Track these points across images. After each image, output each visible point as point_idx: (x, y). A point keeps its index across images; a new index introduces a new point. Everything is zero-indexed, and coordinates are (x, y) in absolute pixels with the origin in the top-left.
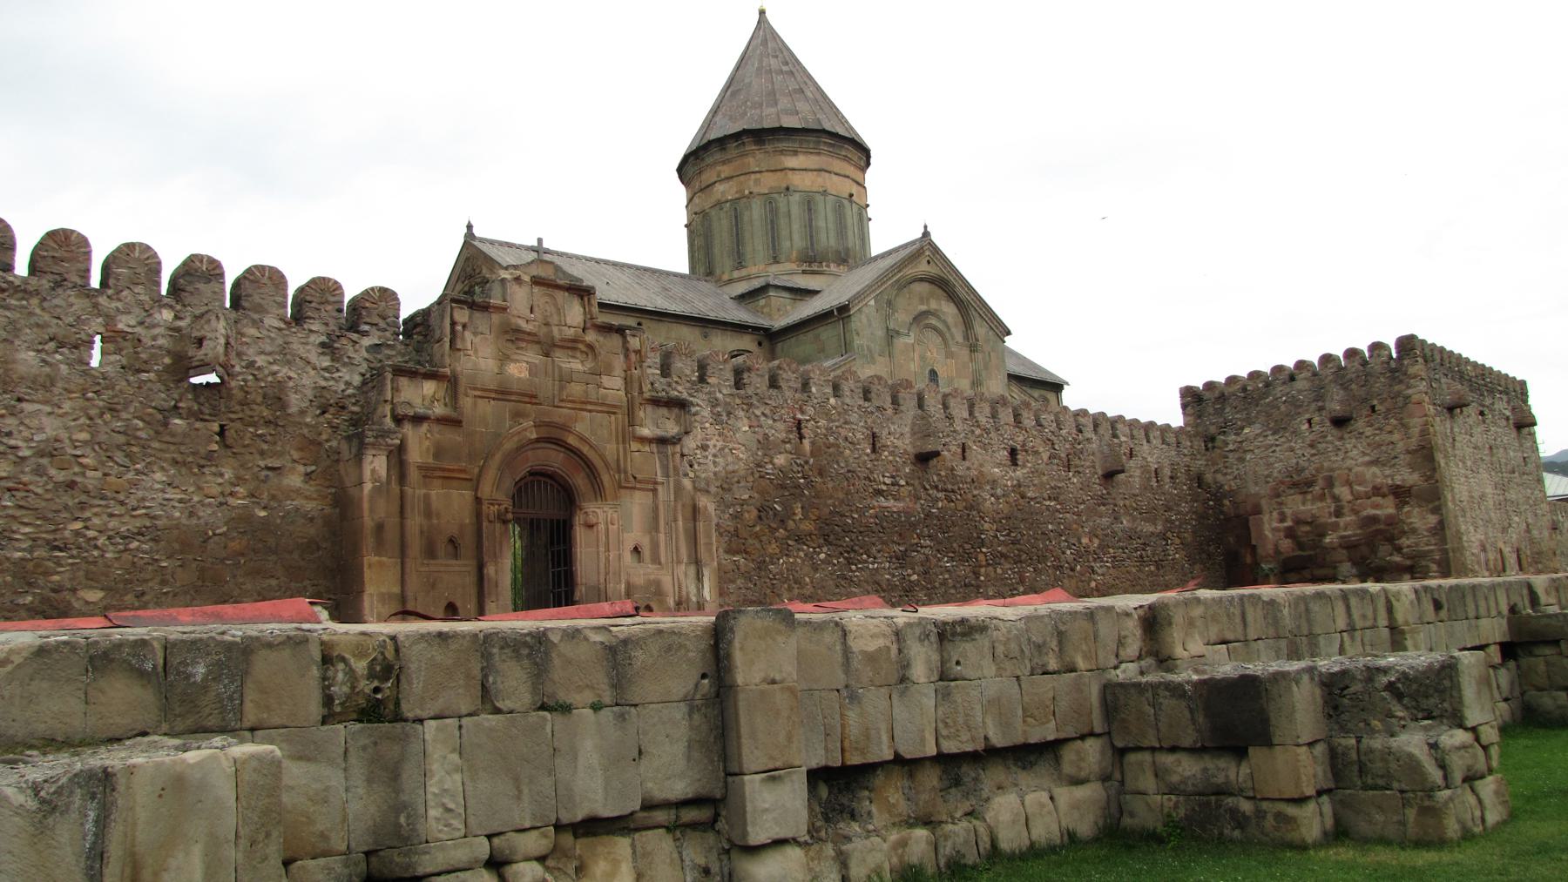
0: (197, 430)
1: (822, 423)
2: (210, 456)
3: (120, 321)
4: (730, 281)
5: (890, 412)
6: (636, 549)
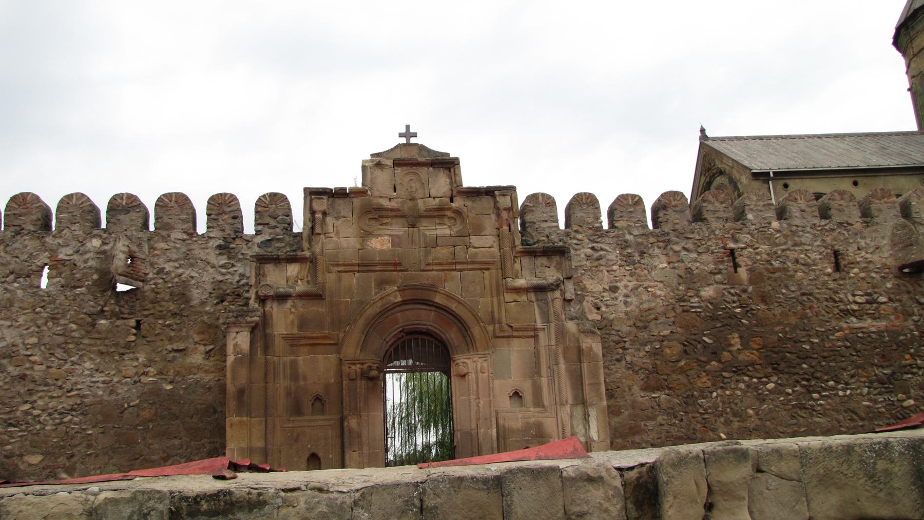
0: (117, 326)
1: (763, 248)
2: (128, 345)
3: (61, 253)
5: (858, 226)
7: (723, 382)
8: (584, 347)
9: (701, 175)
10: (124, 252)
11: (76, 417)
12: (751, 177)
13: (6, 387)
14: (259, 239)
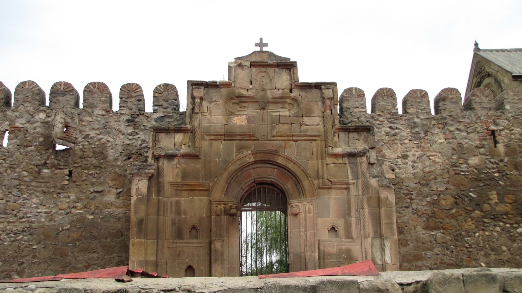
0: (56, 174)
2: (63, 187)
7: (484, 226)
8: (382, 197)
9: (474, 77)
10: (61, 123)
11: (25, 236)
12: (511, 78)
14: (156, 116)
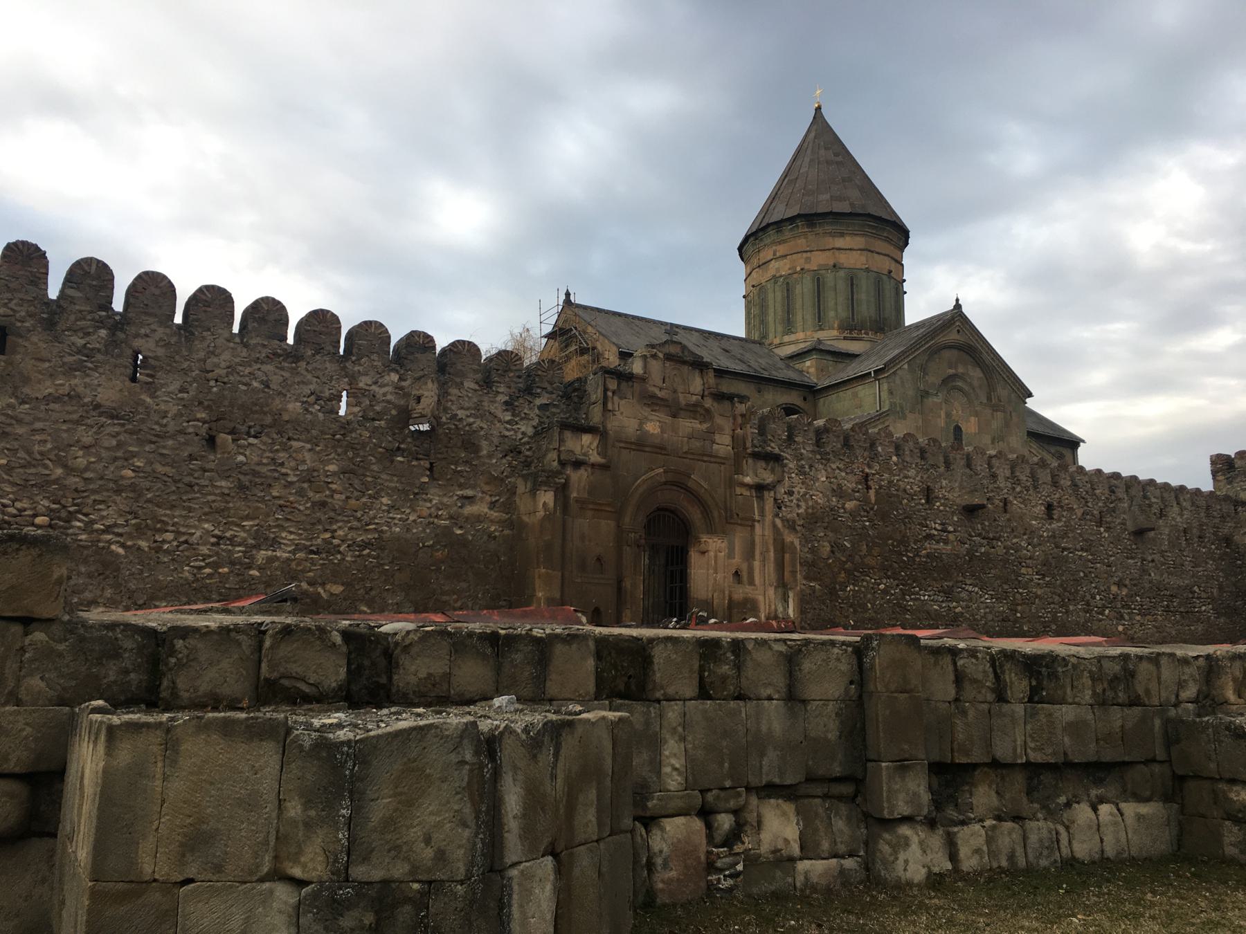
1: (886, 476)
4: (781, 344)
5: (942, 469)
6: (736, 572)
11: (373, 550)
13: (308, 512)
